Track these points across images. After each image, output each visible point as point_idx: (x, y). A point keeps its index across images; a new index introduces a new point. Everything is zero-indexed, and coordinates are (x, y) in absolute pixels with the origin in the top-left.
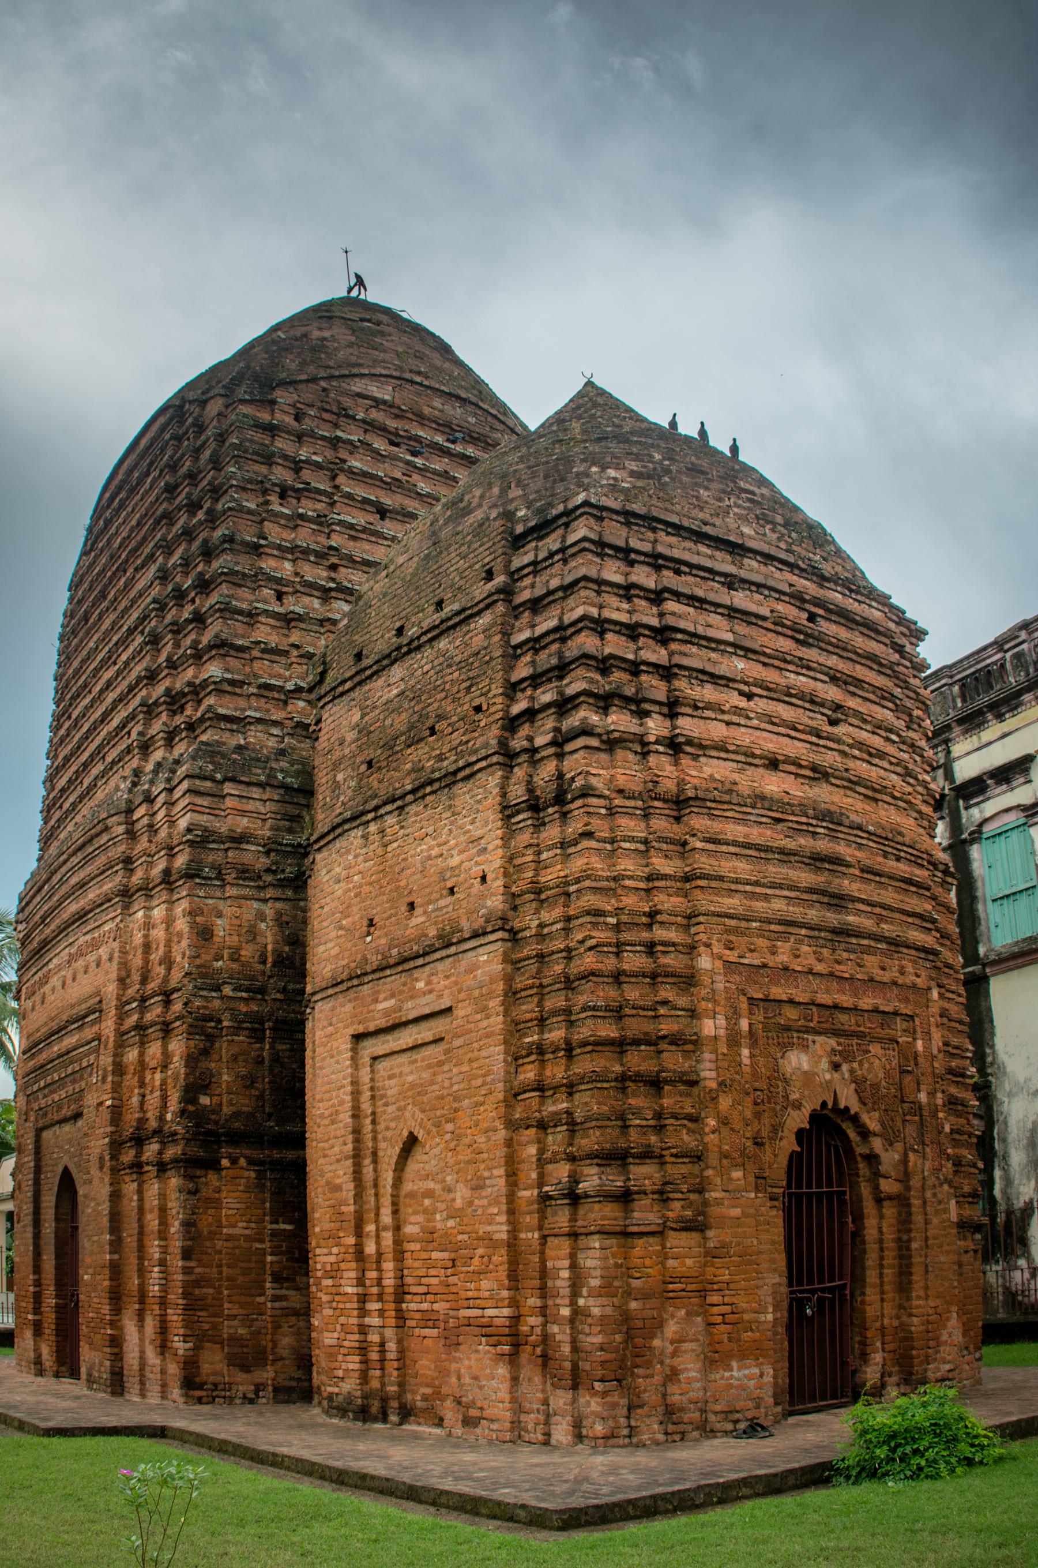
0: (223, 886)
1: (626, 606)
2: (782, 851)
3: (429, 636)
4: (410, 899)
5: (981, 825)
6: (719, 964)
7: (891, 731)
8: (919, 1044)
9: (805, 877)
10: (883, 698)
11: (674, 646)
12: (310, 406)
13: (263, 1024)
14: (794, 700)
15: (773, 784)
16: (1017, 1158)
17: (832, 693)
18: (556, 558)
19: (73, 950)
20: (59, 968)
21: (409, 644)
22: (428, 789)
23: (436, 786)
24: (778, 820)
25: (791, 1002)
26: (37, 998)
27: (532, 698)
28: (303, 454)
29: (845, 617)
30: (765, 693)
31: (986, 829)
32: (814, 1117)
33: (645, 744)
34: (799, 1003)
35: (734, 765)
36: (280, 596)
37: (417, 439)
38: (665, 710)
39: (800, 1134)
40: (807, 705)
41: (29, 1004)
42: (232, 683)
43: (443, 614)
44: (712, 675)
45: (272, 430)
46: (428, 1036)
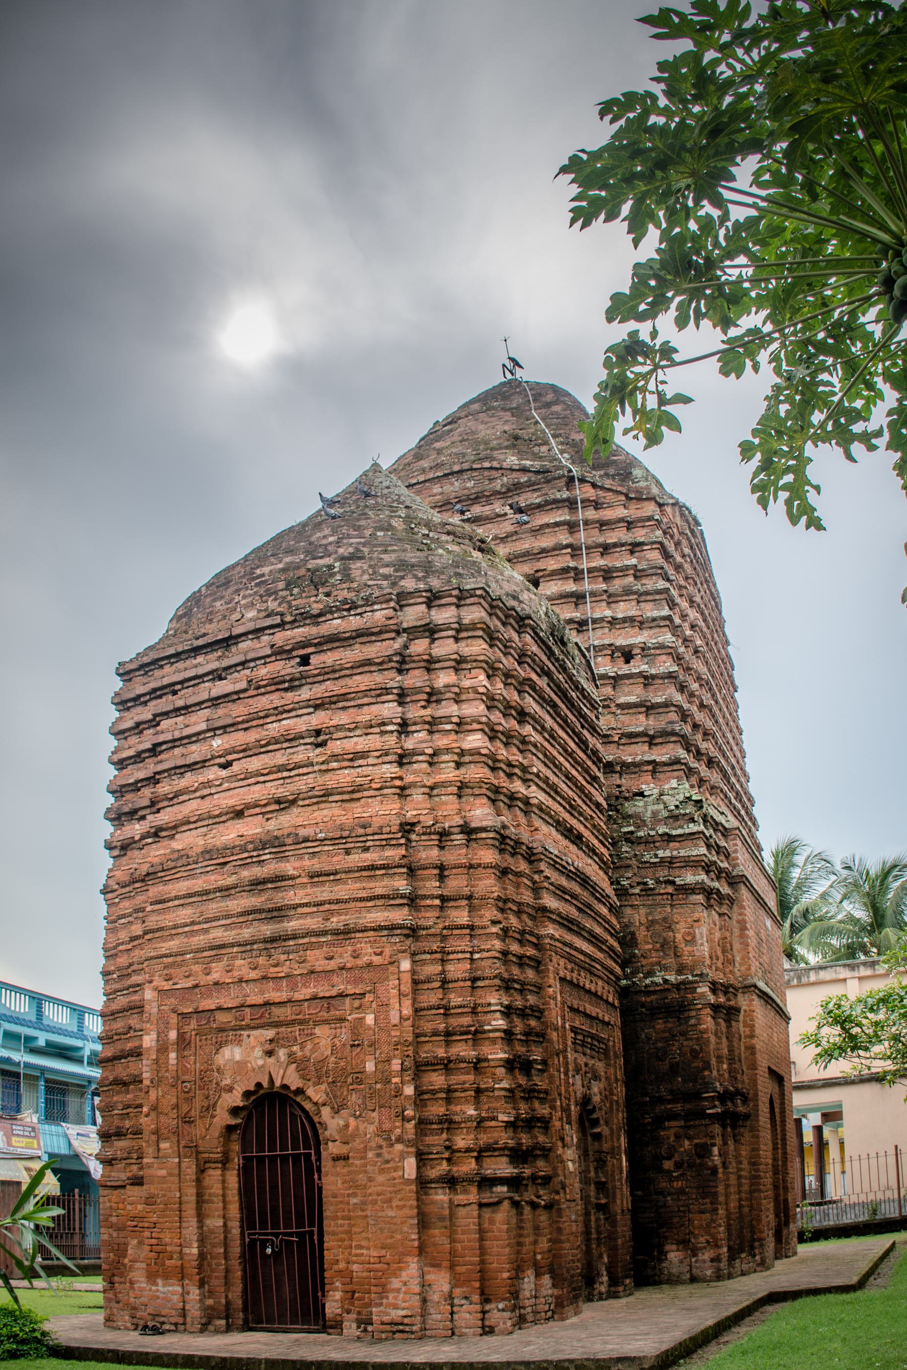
7: (384, 724)
25: (220, 1009)
30: (241, 755)
34: (231, 1008)
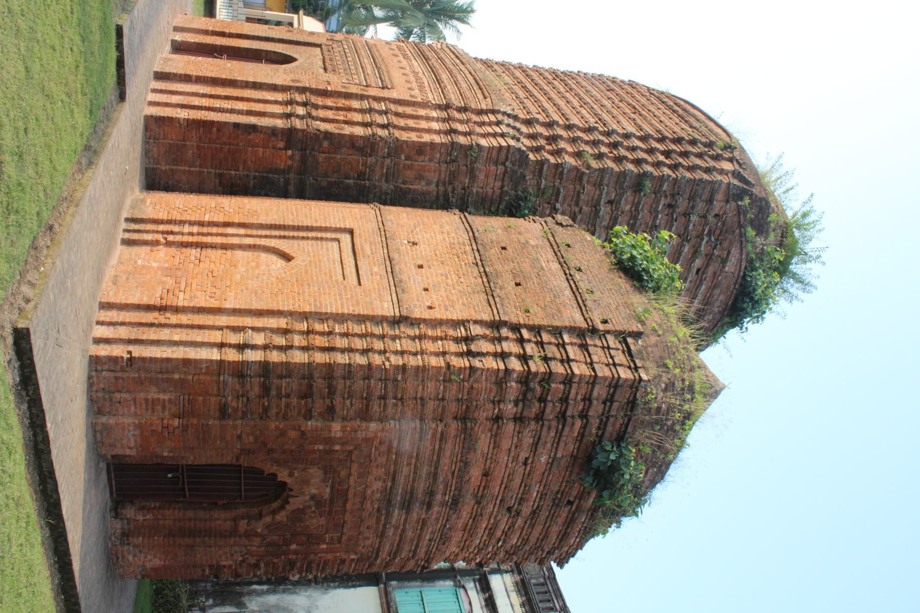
0: (446, 163)
1: (579, 397)
2: (435, 475)
3: (573, 286)
5: (464, 587)
6: (370, 435)
7: (504, 542)
8: (325, 546)
9: (421, 487)
10: (523, 540)
11: (554, 423)
12: (724, 223)
14: (522, 488)
15: (475, 473)
16: (272, 599)
17: (526, 510)
19: (420, 75)
20: (411, 66)
21: (571, 275)
22: (485, 280)
23: (487, 285)
24: (453, 473)
26: (397, 52)
27: (529, 341)
28: (694, 218)
29: (570, 521)
31: (462, 590)
32: (284, 485)
33: (499, 402)
35: (486, 452)
36: (610, 202)
37: (698, 287)
38: (518, 416)
39: (275, 475)
40: (519, 496)
41: (394, 47)
42: (562, 173)
43: (586, 296)
44: (537, 443)
45: (710, 201)
46: (347, 272)
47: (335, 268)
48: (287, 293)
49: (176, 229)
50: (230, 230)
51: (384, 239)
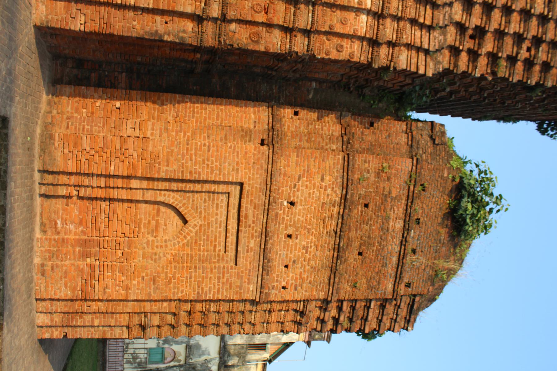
4: (294, 237)
13: (276, 70)
18: (395, 316)
21: (406, 241)
23: (335, 261)
47: (220, 233)
48: (178, 278)
49: (86, 181)
50: (134, 184)
51: (267, 201)
